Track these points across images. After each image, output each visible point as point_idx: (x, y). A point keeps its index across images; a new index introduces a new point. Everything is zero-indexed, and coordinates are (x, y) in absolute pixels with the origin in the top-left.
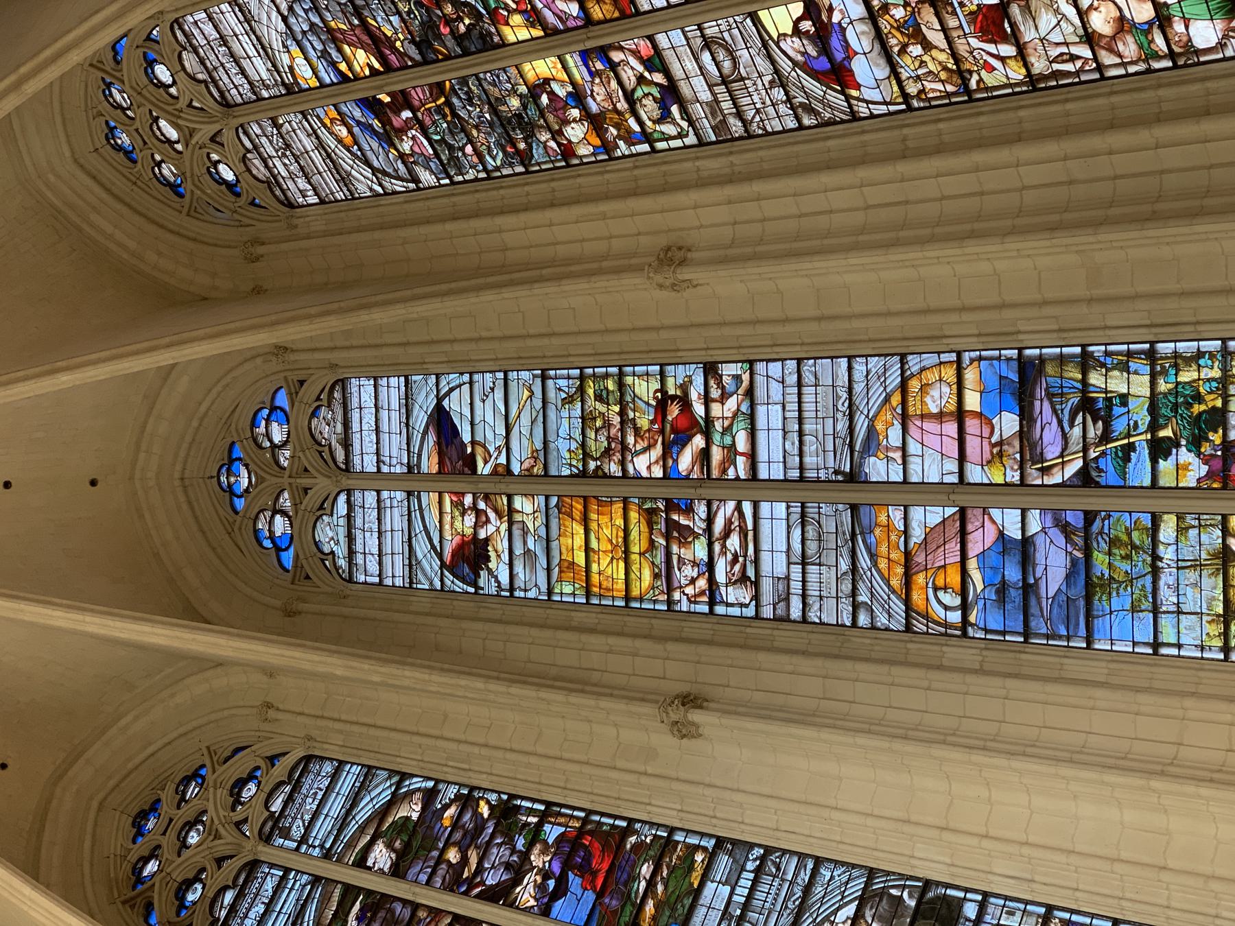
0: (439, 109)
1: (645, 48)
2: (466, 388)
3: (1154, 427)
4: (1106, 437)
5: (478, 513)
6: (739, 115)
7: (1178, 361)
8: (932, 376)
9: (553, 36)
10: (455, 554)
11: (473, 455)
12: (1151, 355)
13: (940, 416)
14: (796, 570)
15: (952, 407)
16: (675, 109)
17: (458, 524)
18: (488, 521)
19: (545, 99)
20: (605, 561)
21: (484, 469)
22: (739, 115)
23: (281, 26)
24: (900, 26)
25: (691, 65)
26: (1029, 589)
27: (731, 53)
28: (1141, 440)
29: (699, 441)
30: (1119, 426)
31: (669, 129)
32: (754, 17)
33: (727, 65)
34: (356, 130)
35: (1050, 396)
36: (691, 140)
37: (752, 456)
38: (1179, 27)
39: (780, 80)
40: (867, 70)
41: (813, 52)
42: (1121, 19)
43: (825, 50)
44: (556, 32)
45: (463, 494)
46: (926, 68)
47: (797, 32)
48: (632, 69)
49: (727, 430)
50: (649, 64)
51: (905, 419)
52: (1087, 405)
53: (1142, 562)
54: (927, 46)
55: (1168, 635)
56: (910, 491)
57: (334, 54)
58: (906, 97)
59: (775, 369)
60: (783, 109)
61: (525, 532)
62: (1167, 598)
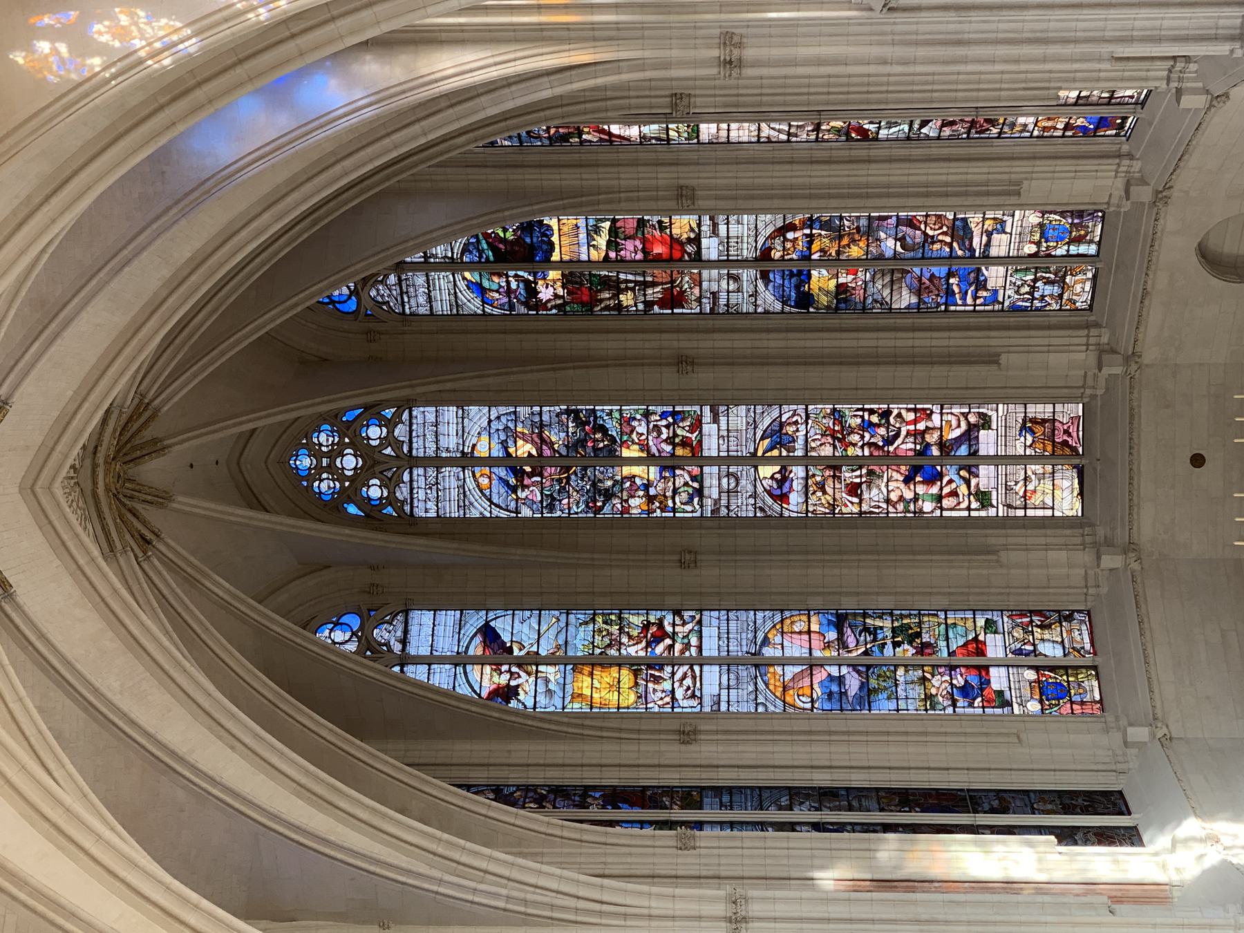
0: (560, 481)
1: (696, 470)
2: (509, 618)
3: (893, 637)
4: (875, 640)
5: (512, 674)
6: (728, 507)
7: (902, 617)
8: (796, 619)
9: (650, 459)
10: (490, 693)
11: (511, 647)
13: (800, 633)
14: (724, 693)
15: (806, 629)
16: (696, 500)
18: (519, 676)
19: (628, 484)
21: (516, 652)
22: (728, 507)
24: (817, 484)
25: (715, 482)
26: (843, 694)
27: (737, 480)
28: (889, 642)
29: (668, 641)
30: (880, 636)
31: (689, 508)
32: (756, 468)
33: (733, 485)
35: (850, 626)
36: (698, 514)
37: (700, 648)
38: (920, 502)
39: (755, 495)
40: (795, 498)
41: (775, 486)
42: (901, 496)
43: (780, 487)
44: (654, 455)
45: (501, 665)
46: (819, 503)
47: (772, 478)
49: (684, 637)
50: (694, 478)
51: (782, 633)
52: (866, 629)
53: (890, 683)
54: (825, 493)
55: (902, 704)
56: (784, 662)
57: (510, 443)
58: (807, 511)
60: (750, 507)
61: (547, 681)
62: (901, 693)
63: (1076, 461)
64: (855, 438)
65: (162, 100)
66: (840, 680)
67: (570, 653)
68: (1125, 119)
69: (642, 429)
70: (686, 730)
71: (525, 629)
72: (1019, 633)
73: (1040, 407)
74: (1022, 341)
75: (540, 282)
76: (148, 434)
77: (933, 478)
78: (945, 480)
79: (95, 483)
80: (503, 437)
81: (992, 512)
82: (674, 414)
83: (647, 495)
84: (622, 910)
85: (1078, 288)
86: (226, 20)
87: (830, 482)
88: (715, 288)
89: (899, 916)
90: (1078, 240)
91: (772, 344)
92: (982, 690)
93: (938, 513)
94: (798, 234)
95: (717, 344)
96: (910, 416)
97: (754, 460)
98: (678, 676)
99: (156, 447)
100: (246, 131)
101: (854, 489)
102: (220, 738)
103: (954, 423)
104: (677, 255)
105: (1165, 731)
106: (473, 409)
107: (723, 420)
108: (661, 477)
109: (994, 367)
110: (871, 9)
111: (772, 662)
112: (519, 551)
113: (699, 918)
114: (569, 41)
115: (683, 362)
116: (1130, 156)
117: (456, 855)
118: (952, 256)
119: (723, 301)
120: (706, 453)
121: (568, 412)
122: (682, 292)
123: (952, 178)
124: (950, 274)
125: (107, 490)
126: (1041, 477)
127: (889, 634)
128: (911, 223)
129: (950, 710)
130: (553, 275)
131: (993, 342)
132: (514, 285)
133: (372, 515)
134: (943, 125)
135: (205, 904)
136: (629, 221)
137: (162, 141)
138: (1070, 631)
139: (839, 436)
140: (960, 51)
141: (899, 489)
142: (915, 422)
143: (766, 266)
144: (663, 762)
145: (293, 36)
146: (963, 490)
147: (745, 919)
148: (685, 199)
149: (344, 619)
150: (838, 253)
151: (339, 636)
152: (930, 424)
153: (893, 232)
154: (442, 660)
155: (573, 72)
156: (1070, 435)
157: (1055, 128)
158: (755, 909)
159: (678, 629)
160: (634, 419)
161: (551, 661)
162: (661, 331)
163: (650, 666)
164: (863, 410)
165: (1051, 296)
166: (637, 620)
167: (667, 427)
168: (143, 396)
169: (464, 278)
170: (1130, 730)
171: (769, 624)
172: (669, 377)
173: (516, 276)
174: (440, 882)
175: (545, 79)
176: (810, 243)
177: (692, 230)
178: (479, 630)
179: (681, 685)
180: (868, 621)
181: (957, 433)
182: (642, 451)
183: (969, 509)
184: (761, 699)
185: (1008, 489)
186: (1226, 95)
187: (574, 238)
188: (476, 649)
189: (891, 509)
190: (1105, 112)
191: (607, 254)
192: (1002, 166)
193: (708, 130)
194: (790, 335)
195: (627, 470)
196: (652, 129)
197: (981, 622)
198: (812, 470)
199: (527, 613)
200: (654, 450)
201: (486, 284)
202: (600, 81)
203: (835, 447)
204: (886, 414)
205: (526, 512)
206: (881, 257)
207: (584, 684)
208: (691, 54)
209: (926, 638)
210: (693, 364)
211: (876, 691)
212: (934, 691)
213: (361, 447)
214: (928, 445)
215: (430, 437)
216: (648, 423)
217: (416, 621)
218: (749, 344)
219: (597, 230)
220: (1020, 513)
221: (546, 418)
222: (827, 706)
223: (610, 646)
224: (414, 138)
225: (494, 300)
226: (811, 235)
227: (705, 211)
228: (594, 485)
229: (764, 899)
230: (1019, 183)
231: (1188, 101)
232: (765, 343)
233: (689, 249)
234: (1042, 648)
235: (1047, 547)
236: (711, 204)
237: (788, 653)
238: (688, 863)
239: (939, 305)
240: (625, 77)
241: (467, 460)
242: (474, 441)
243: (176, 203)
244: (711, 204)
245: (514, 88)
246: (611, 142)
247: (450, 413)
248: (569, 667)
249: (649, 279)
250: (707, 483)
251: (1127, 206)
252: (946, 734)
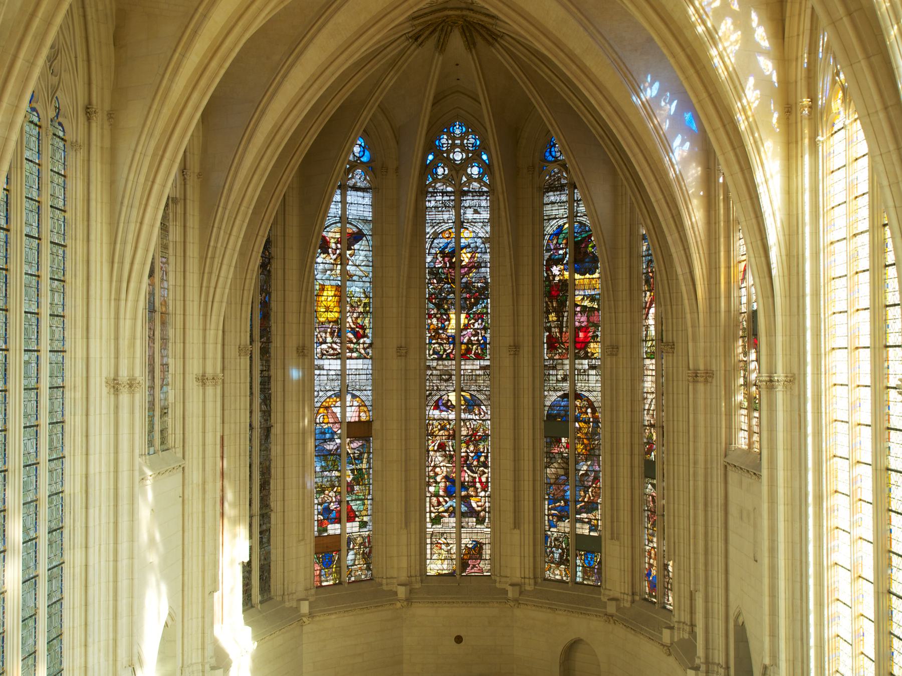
0: (447, 278)
2: (367, 248)
4: (355, 459)
9: (460, 330)
11: (351, 249)
12: (370, 468)
13: (359, 416)
14: (325, 372)
17: (332, 241)
20: (325, 303)
21: (349, 252)
23: (480, 235)
24: (445, 425)
26: (325, 441)
28: (354, 467)
29: (355, 341)
31: (431, 352)
32: (454, 391)
34: (446, 241)
37: (351, 358)
39: (438, 390)
40: (437, 412)
47: (449, 400)
48: (449, 348)
49: (357, 350)
50: (448, 355)
51: (359, 406)
52: (361, 454)
54: (440, 430)
56: (343, 408)
57: (469, 250)
59: (370, 367)
63: (458, 572)
64: (472, 448)
65: (688, 50)
66: (332, 440)
67: (348, 283)
68: (655, 597)
69: (476, 326)
70: (304, 352)
71: (361, 258)
72: (359, 540)
73: (488, 552)
74: (527, 542)
75: (562, 267)
76: (479, 40)
77: (449, 493)
78: (447, 499)
79: (452, 9)
80: (472, 245)
81: (429, 525)
82: (485, 343)
83: (438, 329)
84: (209, 314)
85: (557, 572)
86: (735, 88)
87: (446, 433)
88: (559, 367)
89: (207, 472)
90: (584, 572)
91: (526, 401)
92: (328, 519)
93: (428, 495)
94: (590, 415)
95: (526, 368)
96: (484, 479)
97: (459, 390)
98: (334, 346)
99: (470, 44)
100: (655, 100)
101: (442, 447)
102: (308, 80)
103: (480, 504)
104: (578, 346)
105: (307, 622)
106: (488, 229)
107: (481, 372)
108: (449, 337)
109: (512, 526)
110: (726, 456)
111: (343, 401)
112: (407, 255)
113: (204, 358)
114: (709, 284)
115: (516, 348)
116: (633, 602)
117: (239, 218)
118: (577, 502)
119: (551, 372)
120: (463, 363)
121: (486, 283)
122: (556, 348)
123: (622, 501)
124: (566, 502)
125: (448, 16)
126: (448, 551)
127: (358, 467)
128: (596, 479)
129: (316, 501)
130: (567, 275)
131: (526, 526)
132: (561, 252)
133: (428, 169)
134: (653, 497)
135: (223, 72)
136: (597, 317)
137: (665, 51)
138: (361, 569)
139: (474, 438)
140: (701, 506)
141: (442, 472)
142: (480, 482)
143: (571, 397)
144: (287, 337)
145: (724, 126)
146: (441, 509)
147: (204, 384)
148: (611, 350)
149: (367, 153)
150: (579, 438)
151: (357, 149)
152: (479, 490)
153: (591, 469)
154: (344, 209)
155: (691, 287)
156: (472, 568)
157: (650, 558)
158: (210, 390)
159: (361, 346)
160: (482, 321)
161: (344, 272)
162: (533, 336)
163: (340, 330)
164: (488, 452)
165: (553, 557)
166: (367, 321)
167: (478, 340)
168: (502, 37)
169: (565, 224)
170: (307, 603)
171: (364, 398)
172: (507, 341)
173: (566, 253)
174: (225, 208)
175: (688, 271)
176: (585, 422)
177: (593, 354)
178: (360, 230)
179: (329, 347)
180: (366, 455)
181: (474, 505)
182: (464, 325)
183: (431, 512)
184: (321, 394)
185: (443, 534)
186: (670, 655)
187: (587, 286)
188: (351, 229)
189: (430, 468)
190: (659, 587)
191: (577, 305)
192: (628, 530)
193: (650, 364)
194: (531, 410)
195: (453, 316)
196: (652, 331)
197: (365, 519)
198: (453, 423)
199: (370, 259)
200: (465, 333)
201: (561, 236)
202: (686, 302)
203: (466, 436)
204: (486, 467)
205: (429, 259)
206: (577, 463)
207: (329, 293)
208: (701, 353)
209: (356, 488)
210: (515, 354)
211: (326, 460)
212: (327, 492)
213: (466, 163)
214: (467, 489)
215: (472, 203)
216: (480, 329)
217: (366, 194)
218: (526, 386)
219: (592, 298)
220: (428, 541)
221: (483, 270)
222: (317, 431)
223: (352, 306)
224: (655, 195)
225: (552, 240)
226: (589, 422)
227: (603, 362)
228: (445, 298)
229: (215, 395)
230: (618, 539)
231: (666, 633)
232: (526, 396)
233: (582, 353)
234: (351, 553)
235: (409, 556)
236: (608, 365)
237: (348, 409)
238: (232, 351)
239: (548, 495)
240: (688, 316)
241: (460, 224)
242: (470, 229)
243: (619, 58)
244: (608, 365)
245: (683, 252)
246: (645, 308)
247: (485, 215)
248: (339, 283)
249: (564, 329)
250: (446, 362)
251: (604, 599)
252: (304, 499)
